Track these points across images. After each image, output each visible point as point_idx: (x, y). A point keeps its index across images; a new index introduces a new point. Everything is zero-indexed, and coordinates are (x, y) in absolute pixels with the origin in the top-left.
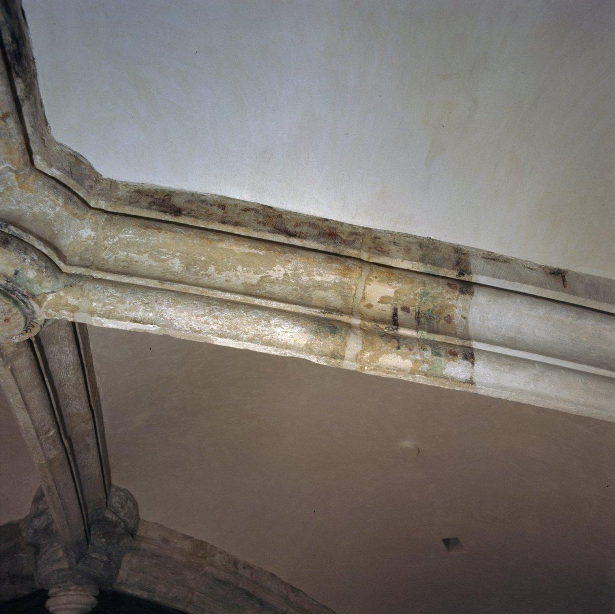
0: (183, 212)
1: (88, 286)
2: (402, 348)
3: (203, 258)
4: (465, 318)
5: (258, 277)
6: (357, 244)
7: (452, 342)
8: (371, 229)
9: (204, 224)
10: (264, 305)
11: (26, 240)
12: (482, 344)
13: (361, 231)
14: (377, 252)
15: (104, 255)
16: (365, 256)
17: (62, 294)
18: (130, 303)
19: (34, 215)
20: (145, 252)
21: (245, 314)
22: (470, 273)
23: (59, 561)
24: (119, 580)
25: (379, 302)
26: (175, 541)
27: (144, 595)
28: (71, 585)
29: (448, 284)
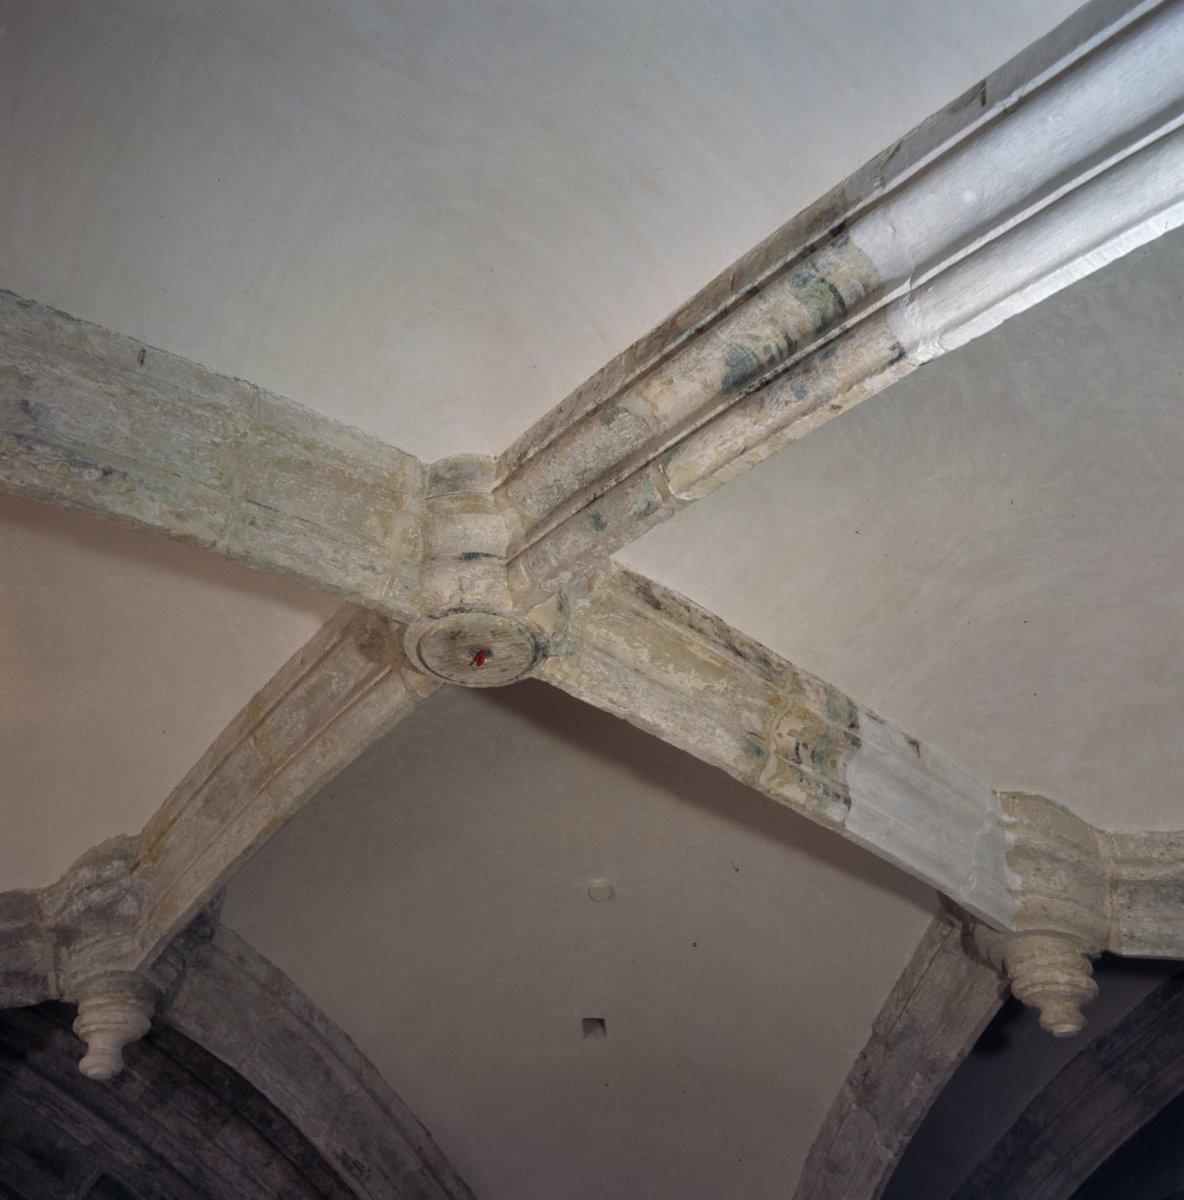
24: (176, 1004)
28: (128, 998)
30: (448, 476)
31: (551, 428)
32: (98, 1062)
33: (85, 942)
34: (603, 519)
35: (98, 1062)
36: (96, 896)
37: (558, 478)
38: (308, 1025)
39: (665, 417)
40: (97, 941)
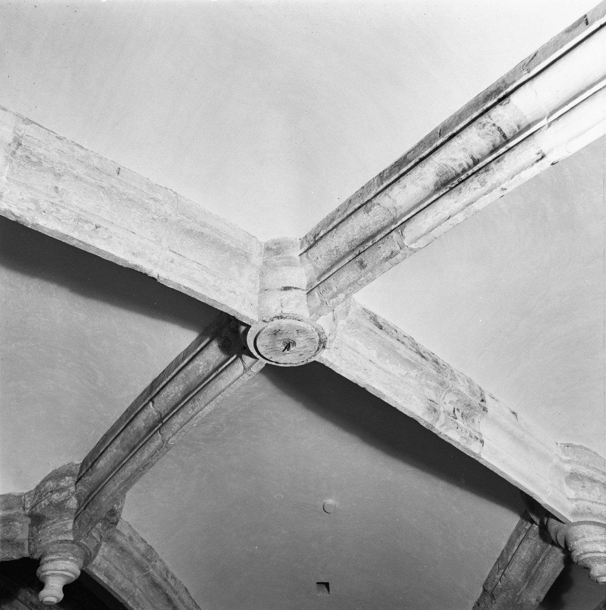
23: (66, 533)
24: (94, 563)
26: (137, 541)
30: (274, 247)
31: (333, 220)
33: (47, 523)
34: (365, 263)
36: (55, 497)
37: (337, 245)
38: (165, 580)
39: (401, 207)
40: (54, 523)
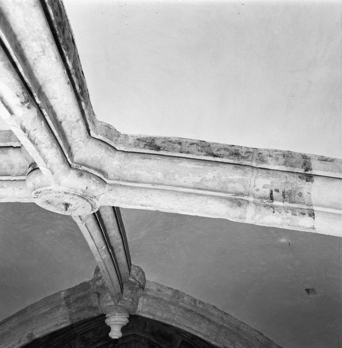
0: (161, 149)
1: (119, 189)
2: (275, 212)
3: (172, 171)
4: (309, 193)
5: (200, 179)
6: (250, 158)
7: (302, 207)
8: (257, 149)
9: (171, 154)
10: (204, 193)
11: (90, 172)
12: (319, 207)
13: (251, 150)
14: (261, 162)
15: (125, 173)
16: (254, 164)
17: (107, 194)
18: (139, 197)
19: (92, 159)
20: (144, 170)
21: (195, 199)
22: (311, 170)
23: (109, 301)
24: (138, 310)
25: (263, 188)
26: (164, 290)
27: (151, 317)
29: (299, 177)
32: (115, 333)
35: (115, 333)
